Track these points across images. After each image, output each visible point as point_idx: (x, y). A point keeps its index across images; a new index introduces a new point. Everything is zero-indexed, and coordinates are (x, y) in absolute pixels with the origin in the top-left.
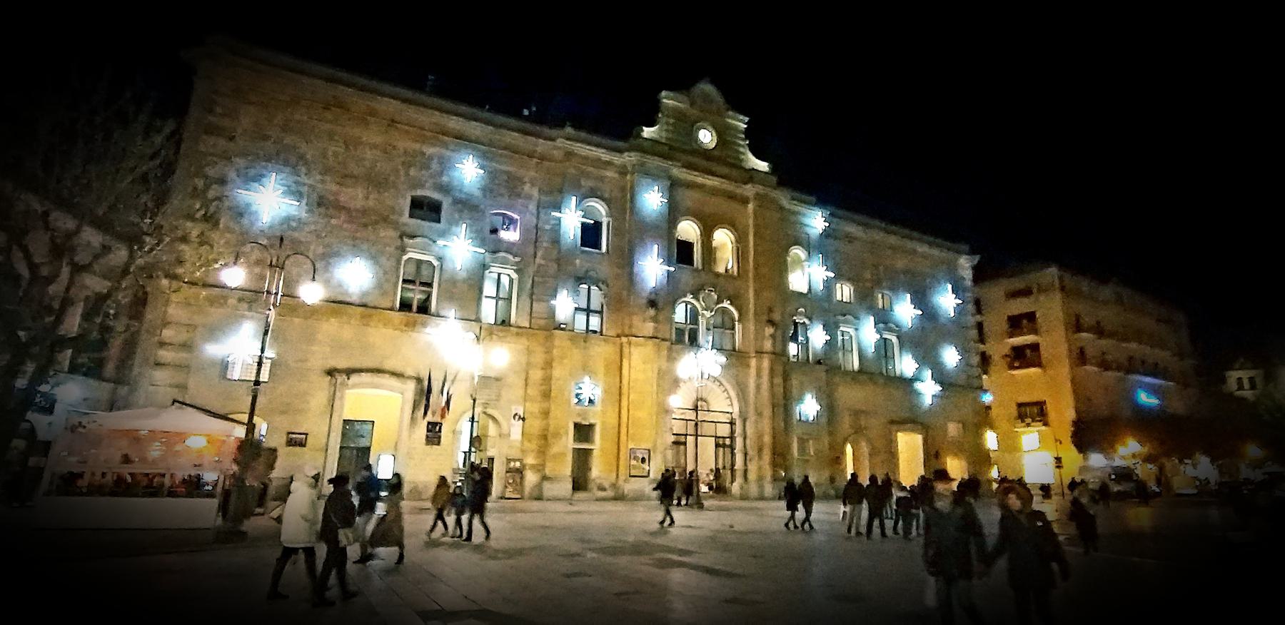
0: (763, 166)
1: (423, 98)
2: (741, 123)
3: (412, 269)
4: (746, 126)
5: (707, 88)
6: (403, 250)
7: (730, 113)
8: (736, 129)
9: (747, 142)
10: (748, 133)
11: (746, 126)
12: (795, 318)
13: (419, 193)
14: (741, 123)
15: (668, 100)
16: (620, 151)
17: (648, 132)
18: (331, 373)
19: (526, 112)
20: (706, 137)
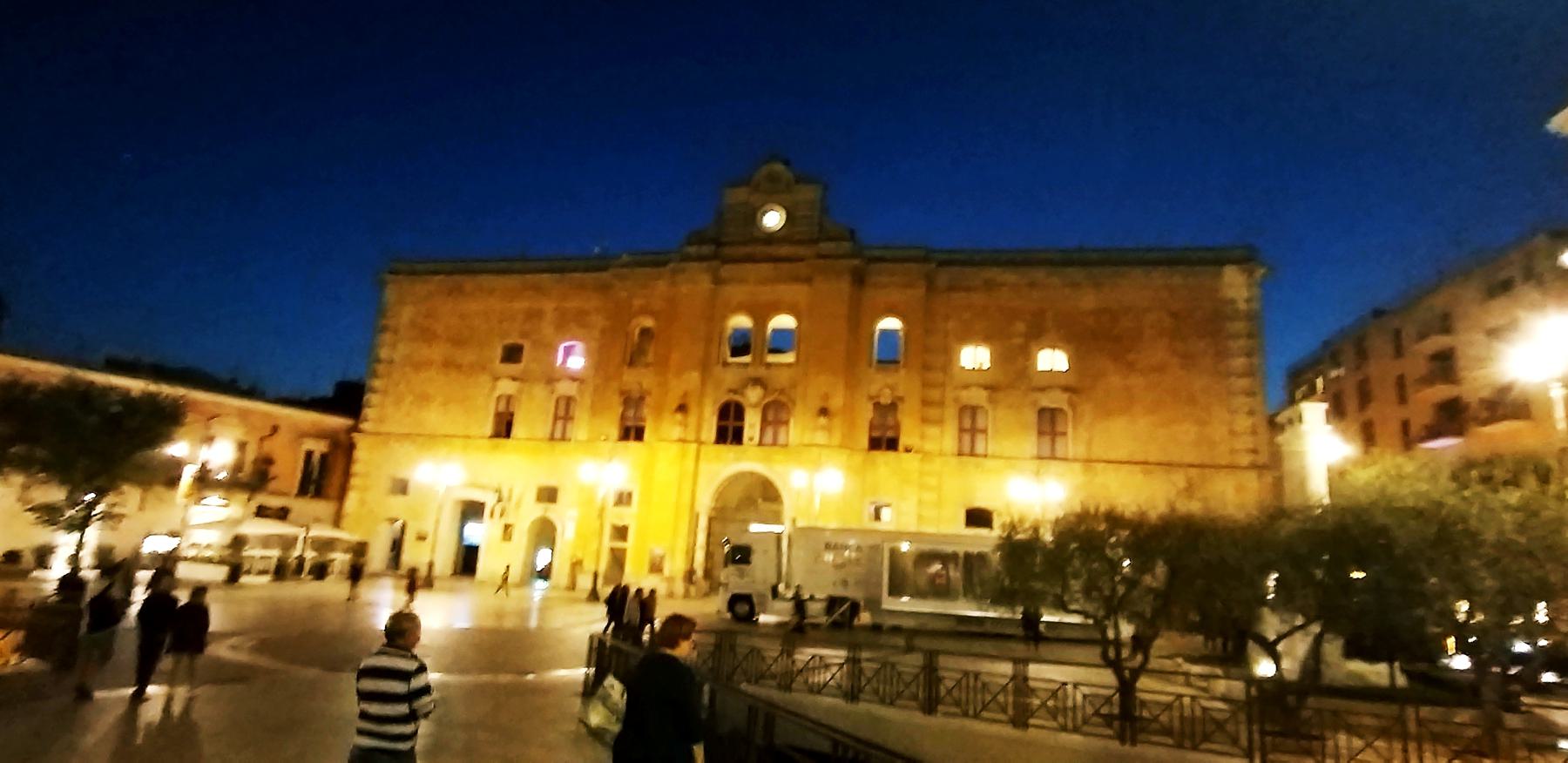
13: (510, 341)
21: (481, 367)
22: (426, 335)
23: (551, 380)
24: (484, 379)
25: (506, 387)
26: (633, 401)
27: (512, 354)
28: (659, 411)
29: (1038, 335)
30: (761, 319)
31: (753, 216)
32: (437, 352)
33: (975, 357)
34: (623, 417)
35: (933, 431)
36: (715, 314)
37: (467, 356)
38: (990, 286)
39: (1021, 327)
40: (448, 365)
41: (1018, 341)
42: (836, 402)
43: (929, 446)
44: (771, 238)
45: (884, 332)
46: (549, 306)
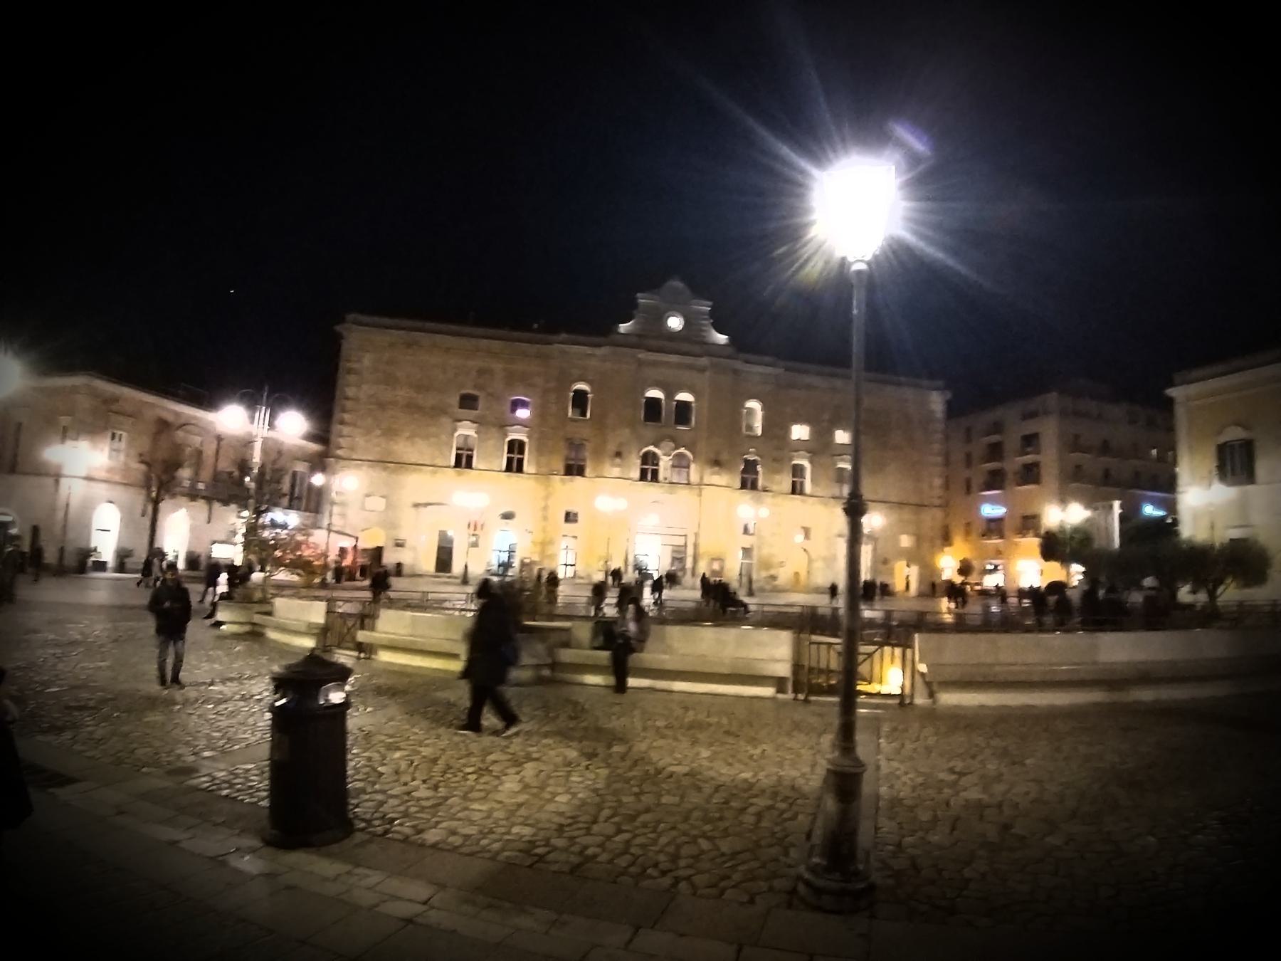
0: (722, 339)
1: (467, 329)
2: (705, 307)
3: (462, 440)
4: (709, 309)
5: (677, 284)
6: (455, 430)
7: (695, 301)
8: (703, 313)
9: (712, 321)
10: (712, 314)
11: (709, 309)
12: (745, 456)
13: (464, 391)
14: (705, 307)
15: (643, 300)
16: (599, 346)
17: (623, 327)
18: (416, 505)
19: (536, 326)
20: (675, 323)
21: (438, 412)
22: (390, 381)
23: (503, 426)
24: (445, 420)
25: (466, 430)
26: (575, 446)
27: (468, 402)
28: (599, 454)
29: (837, 423)
30: (670, 395)
31: (661, 318)
32: (402, 394)
33: (800, 432)
34: (567, 459)
35: (778, 477)
36: (565, 380)
37: (429, 400)
38: (809, 387)
39: (826, 416)
40: (412, 408)
41: (825, 424)
42: (724, 456)
43: (775, 488)
44: (673, 336)
45: (576, 392)
46: (498, 366)
